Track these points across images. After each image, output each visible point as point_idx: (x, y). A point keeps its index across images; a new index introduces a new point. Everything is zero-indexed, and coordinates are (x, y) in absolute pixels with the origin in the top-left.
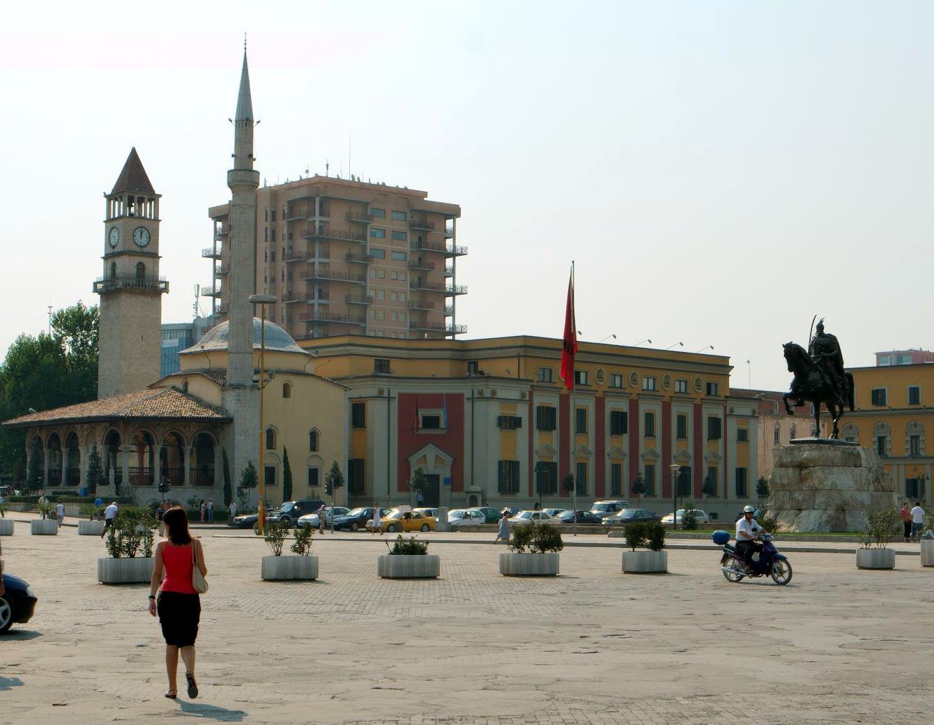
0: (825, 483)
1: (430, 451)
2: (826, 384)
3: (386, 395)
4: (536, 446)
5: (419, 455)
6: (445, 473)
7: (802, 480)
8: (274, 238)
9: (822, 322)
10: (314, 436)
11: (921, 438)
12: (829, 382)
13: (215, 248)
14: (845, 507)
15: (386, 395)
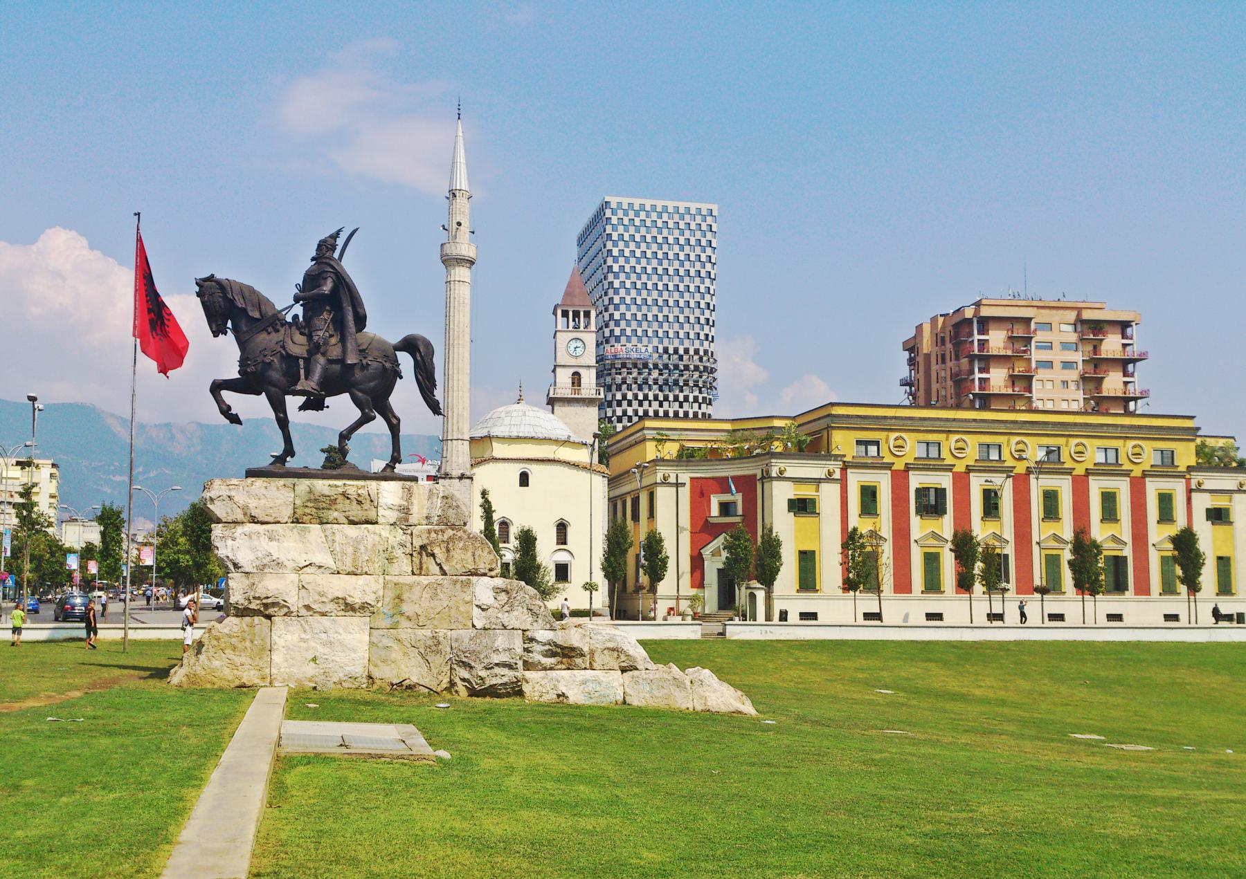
8: (944, 362)
14: (271, 611)
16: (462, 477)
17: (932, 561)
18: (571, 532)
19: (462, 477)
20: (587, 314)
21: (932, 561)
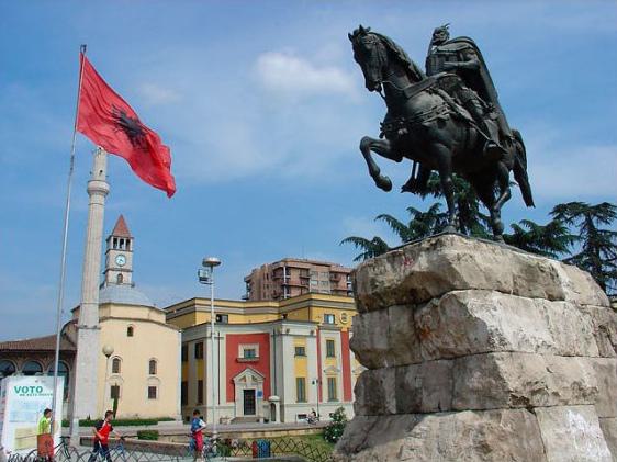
0: (472, 336)
1: (248, 373)
2: (458, 119)
4: (324, 368)
5: (241, 375)
6: (259, 388)
7: (420, 334)
10: (153, 363)
14: (535, 400)
16: (95, 328)
17: (332, 382)
18: (159, 366)
19: (95, 328)
20: (128, 242)
21: (332, 382)
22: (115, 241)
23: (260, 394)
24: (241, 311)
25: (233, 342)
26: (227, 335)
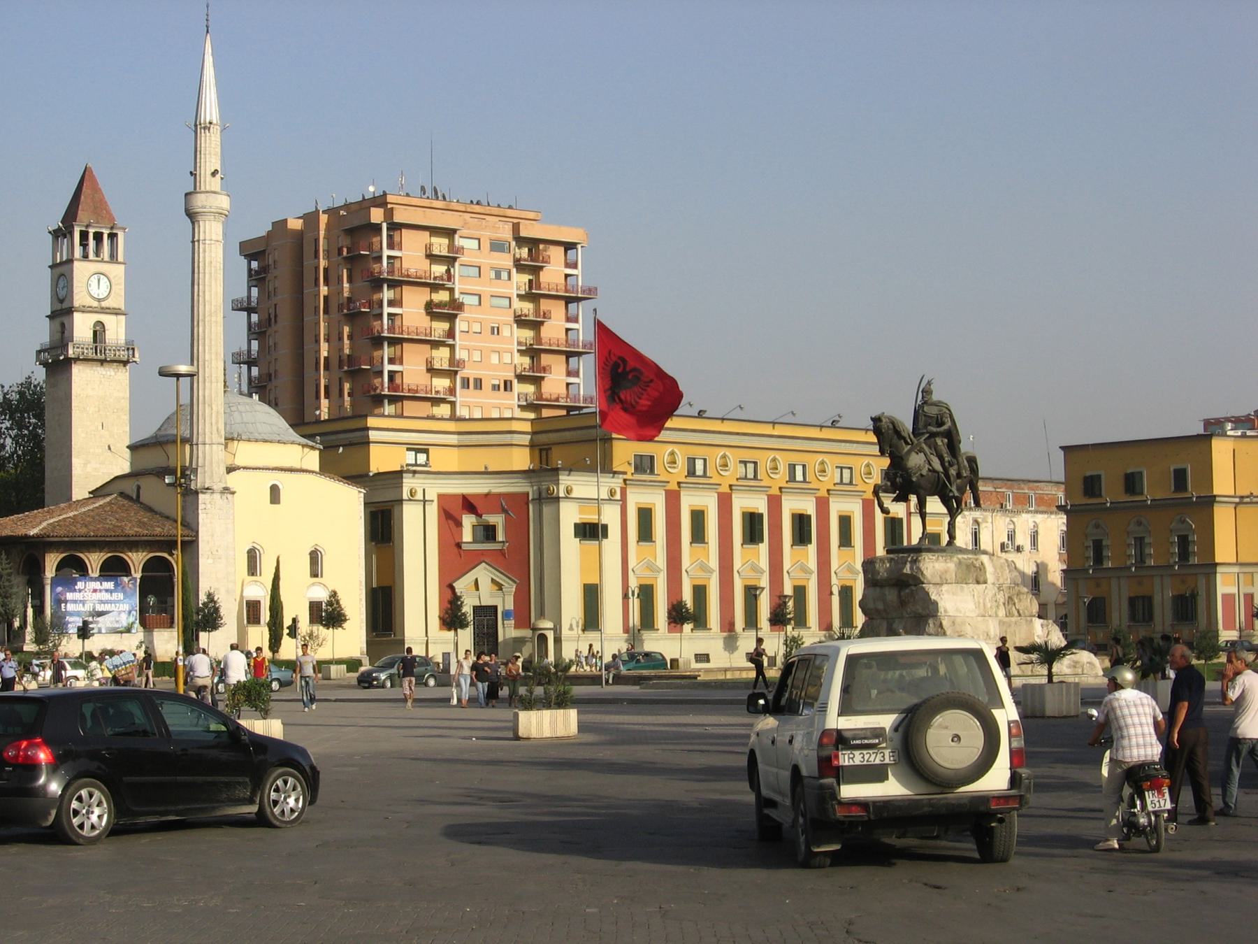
1: (483, 573)
2: (934, 471)
3: (419, 496)
4: (632, 562)
5: (468, 579)
6: (505, 602)
7: (903, 603)
9: (929, 383)
11: (1147, 540)
12: (938, 467)
13: (249, 297)
15: (419, 496)
20: (113, 236)
22: (84, 235)
23: (506, 615)
24: (453, 439)
25: (453, 510)
26: (440, 496)
